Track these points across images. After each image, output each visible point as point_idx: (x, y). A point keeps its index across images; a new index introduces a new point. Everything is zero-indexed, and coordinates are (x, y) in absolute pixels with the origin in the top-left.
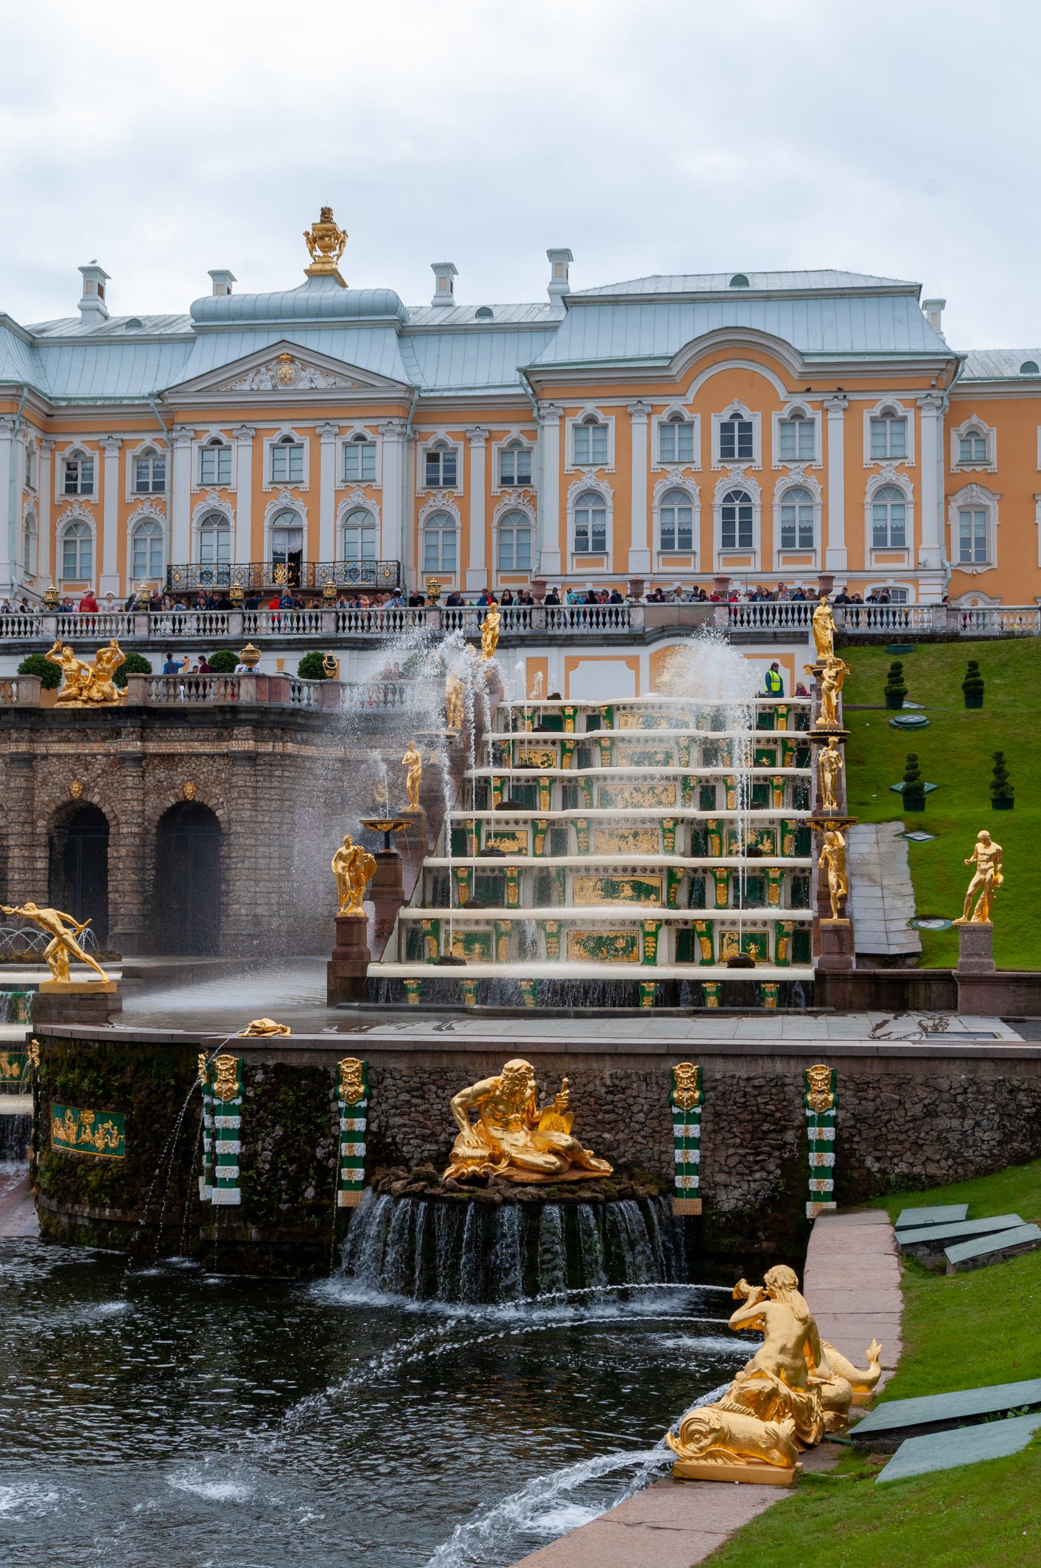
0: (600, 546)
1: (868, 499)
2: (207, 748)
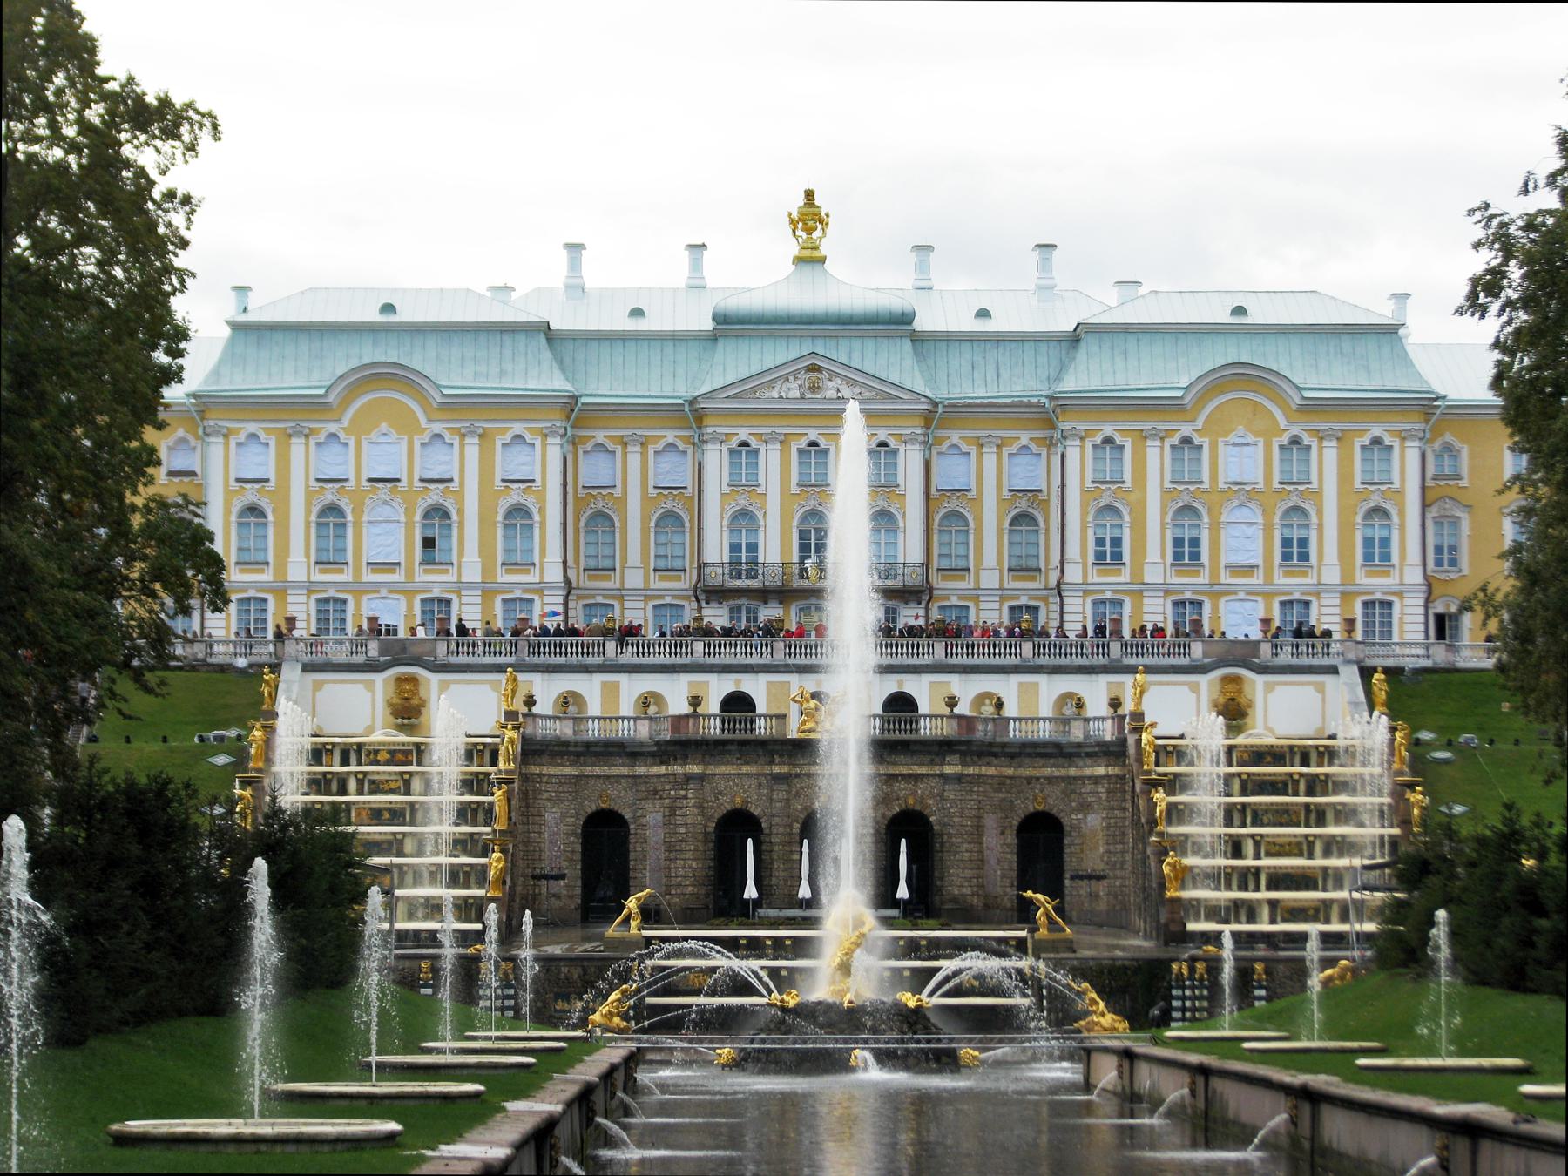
0: (1117, 556)
1: (1359, 519)
2: (924, 770)
